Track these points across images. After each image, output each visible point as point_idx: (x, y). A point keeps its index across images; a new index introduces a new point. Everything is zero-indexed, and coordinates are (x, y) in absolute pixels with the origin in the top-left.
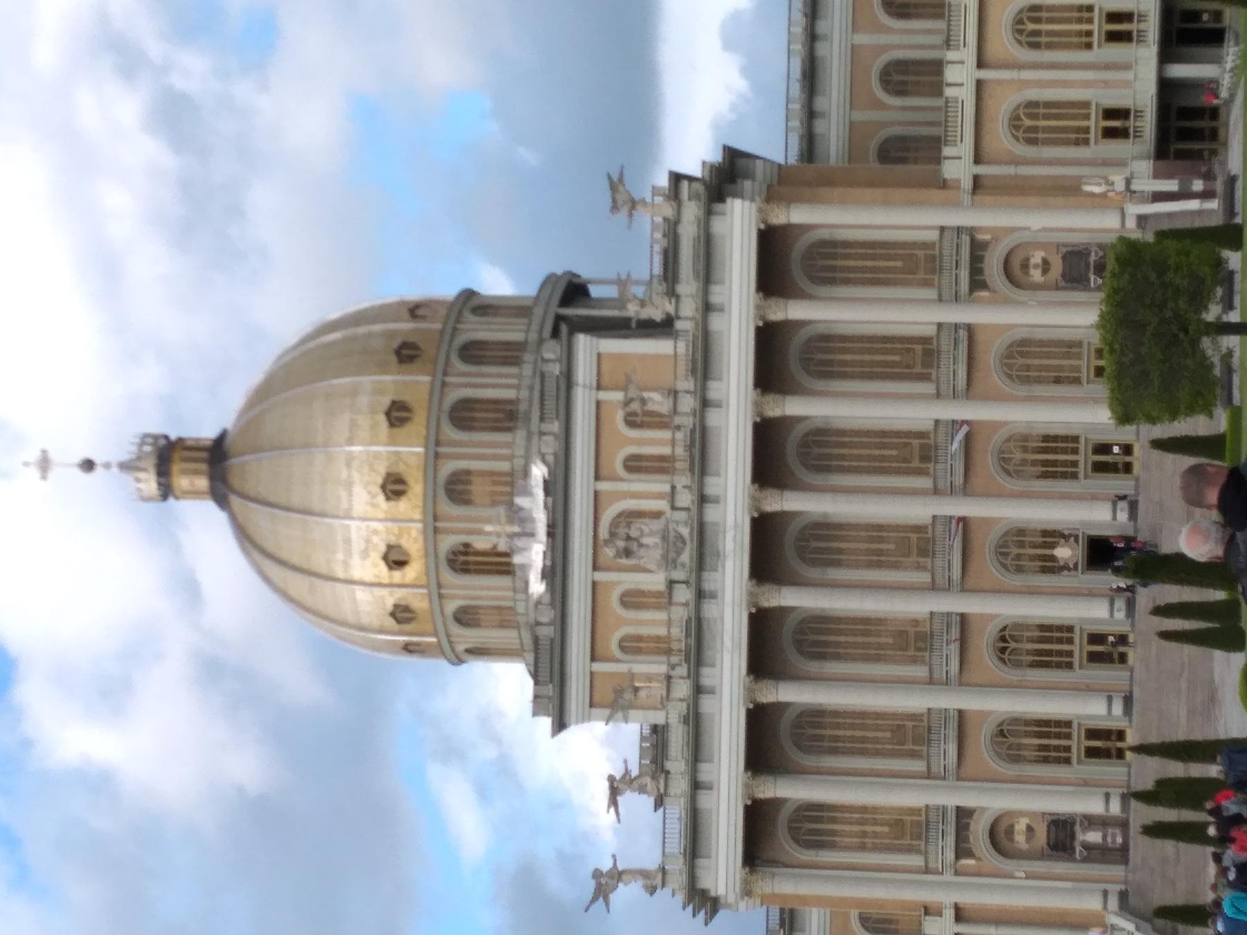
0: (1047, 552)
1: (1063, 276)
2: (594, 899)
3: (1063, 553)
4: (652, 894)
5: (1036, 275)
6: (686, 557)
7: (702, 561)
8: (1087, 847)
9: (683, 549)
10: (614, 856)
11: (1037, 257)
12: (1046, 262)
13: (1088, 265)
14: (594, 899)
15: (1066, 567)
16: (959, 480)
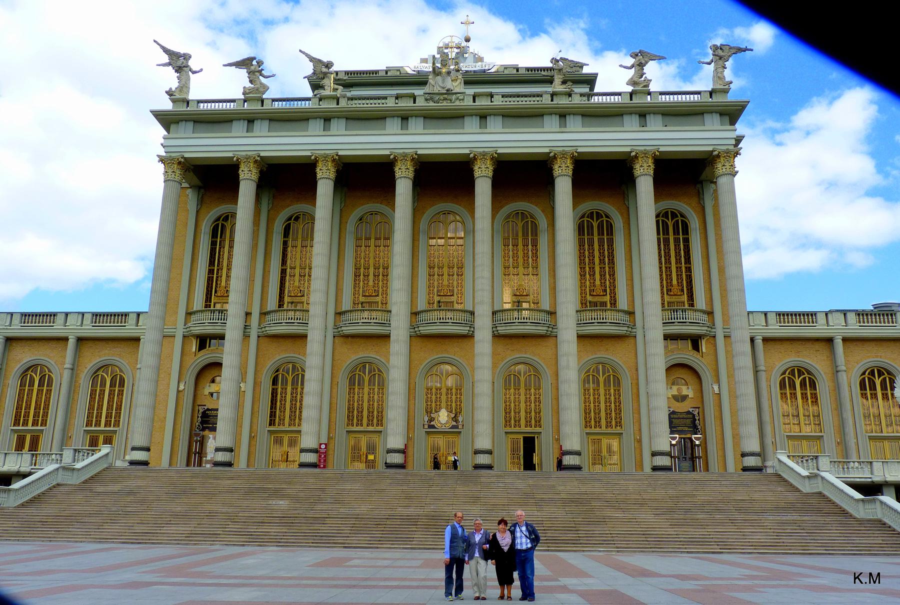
0: (443, 404)
1: (674, 412)
2: (166, 51)
4: (167, 92)
5: (674, 391)
8: (202, 442)
10: (202, 70)
14: (166, 51)
15: (431, 420)
16: (502, 330)
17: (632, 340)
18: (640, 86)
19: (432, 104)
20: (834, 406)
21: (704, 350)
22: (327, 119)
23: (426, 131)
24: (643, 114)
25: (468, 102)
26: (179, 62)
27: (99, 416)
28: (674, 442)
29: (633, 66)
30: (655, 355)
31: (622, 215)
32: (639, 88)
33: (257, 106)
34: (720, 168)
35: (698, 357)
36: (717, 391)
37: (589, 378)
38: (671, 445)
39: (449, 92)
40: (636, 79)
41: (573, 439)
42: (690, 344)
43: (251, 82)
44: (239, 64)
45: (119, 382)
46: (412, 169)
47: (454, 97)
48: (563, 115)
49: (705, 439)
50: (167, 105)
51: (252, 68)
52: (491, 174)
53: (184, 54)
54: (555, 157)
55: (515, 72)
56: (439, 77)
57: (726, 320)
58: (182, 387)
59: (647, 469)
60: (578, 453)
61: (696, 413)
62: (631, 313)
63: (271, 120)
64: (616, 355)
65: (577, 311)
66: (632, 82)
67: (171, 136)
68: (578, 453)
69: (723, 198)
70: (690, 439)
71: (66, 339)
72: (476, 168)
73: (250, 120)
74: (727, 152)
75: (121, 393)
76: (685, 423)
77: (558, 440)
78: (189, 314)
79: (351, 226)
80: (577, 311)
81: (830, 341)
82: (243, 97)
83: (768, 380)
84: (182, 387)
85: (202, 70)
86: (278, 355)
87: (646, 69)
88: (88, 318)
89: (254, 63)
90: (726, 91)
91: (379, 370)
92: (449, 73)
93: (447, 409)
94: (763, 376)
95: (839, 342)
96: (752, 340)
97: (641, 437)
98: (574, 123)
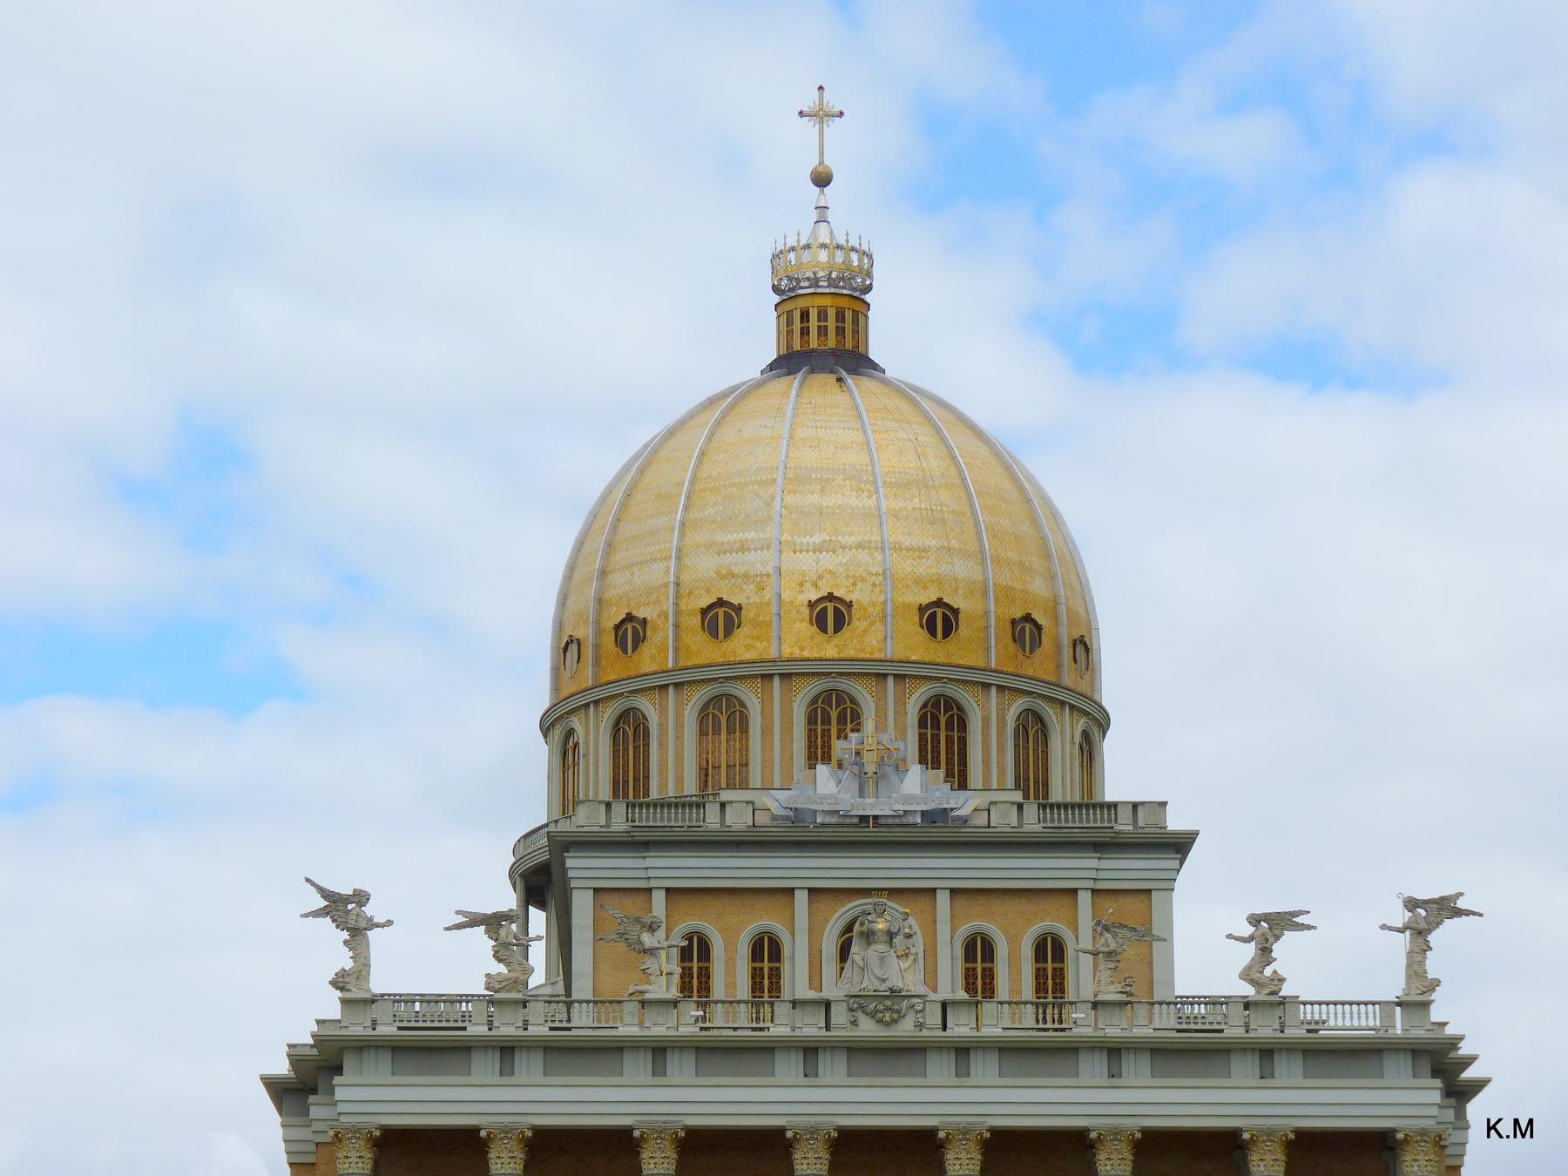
4: (334, 983)
6: (868, 1029)
7: (862, 1054)
9: (880, 1021)
10: (389, 923)
23: (853, 1081)
26: (344, 909)
44: (474, 921)
47: (905, 1004)
66: (1246, 975)
85: (389, 923)
87: (1278, 949)
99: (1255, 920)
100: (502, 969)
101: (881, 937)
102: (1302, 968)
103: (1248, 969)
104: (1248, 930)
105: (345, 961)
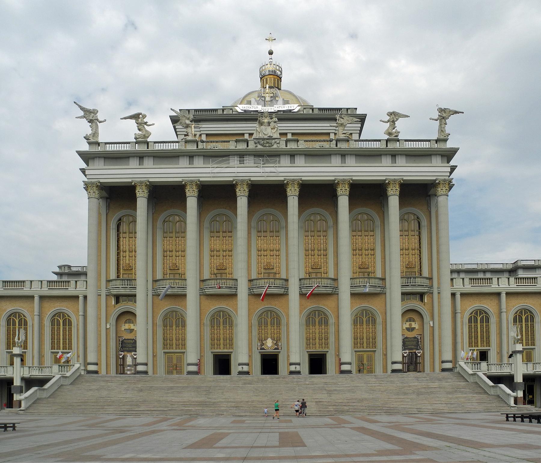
0: (269, 335)
1: (406, 338)
2: (82, 109)
3: (269, 343)
5: (407, 325)
8: (124, 358)
10: (105, 120)
11: (414, 325)
12: (413, 329)
13: (412, 349)
15: (263, 344)
17: (383, 296)
18: (393, 138)
19: (259, 147)
20: (498, 332)
21: (426, 301)
22: (191, 156)
24: (394, 155)
25: (283, 146)
26: (91, 116)
27: (59, 342)
28: (405, 355)
29: (388, 121)
30: (396, 305)
31: (379, 217)
32: (392, 137)
33: (143, 148)
34: (441, 190)
35: (424, 306)
36: (432, 325)
37: (357, 321)
38: (403, 356)
39: (271, 138)
40: (390, 131)
41: (347, 355)
42: (417, 296)
43: (139, 130)
44: (131, 117)
45: (68, 323)
46: (247, 190)
47: (273, 141)
48: (343, 155)
49: (423, 353)
50: (85, 147)
51: (140, 120)
52: (297, 194)
53: (94, 110)
54: (338, 183)
55: (311, 112)
56: (263, 127)
57: (439, 283)
58: (108, 327)
59: (389, 371)
60: (350, 364)
61: (419, 338)
62: (383, 279)
63: (154, 157)
64: (374, 305)
65: (351, 279)
67: (89, 168)
68: (350, 364)
69: (441, 210)
70: (415, 352)
71: (33, 297)
72: (288, 190)
73: (141, 157)
74: (445, 180)
75: (70, 330)
76: (412, 344)
77: (338, 355)
78: (108, 281)
79: (206, 224)
80: (351, 279)
81: (499, 294)
82: (135, 141)
83: (462, 318)
84: (108, 327)
85: (105, 120)
86: (166, 306)
88: (45, 284)
89: (141, 116)
90: (445, 140)
91: (229, 316)
92: (269, 123)
93: (271, 338)
94: (459, 316)
95: (503, 296)
96: (453, 295)
97: (386, 353)
98: (351, 160)
99: (390, 114)
100: (140, 132)
101: (266, 124)
102: (405, 130)
103: (388, 130)
104: (388, 118)
105: (89, 131)
